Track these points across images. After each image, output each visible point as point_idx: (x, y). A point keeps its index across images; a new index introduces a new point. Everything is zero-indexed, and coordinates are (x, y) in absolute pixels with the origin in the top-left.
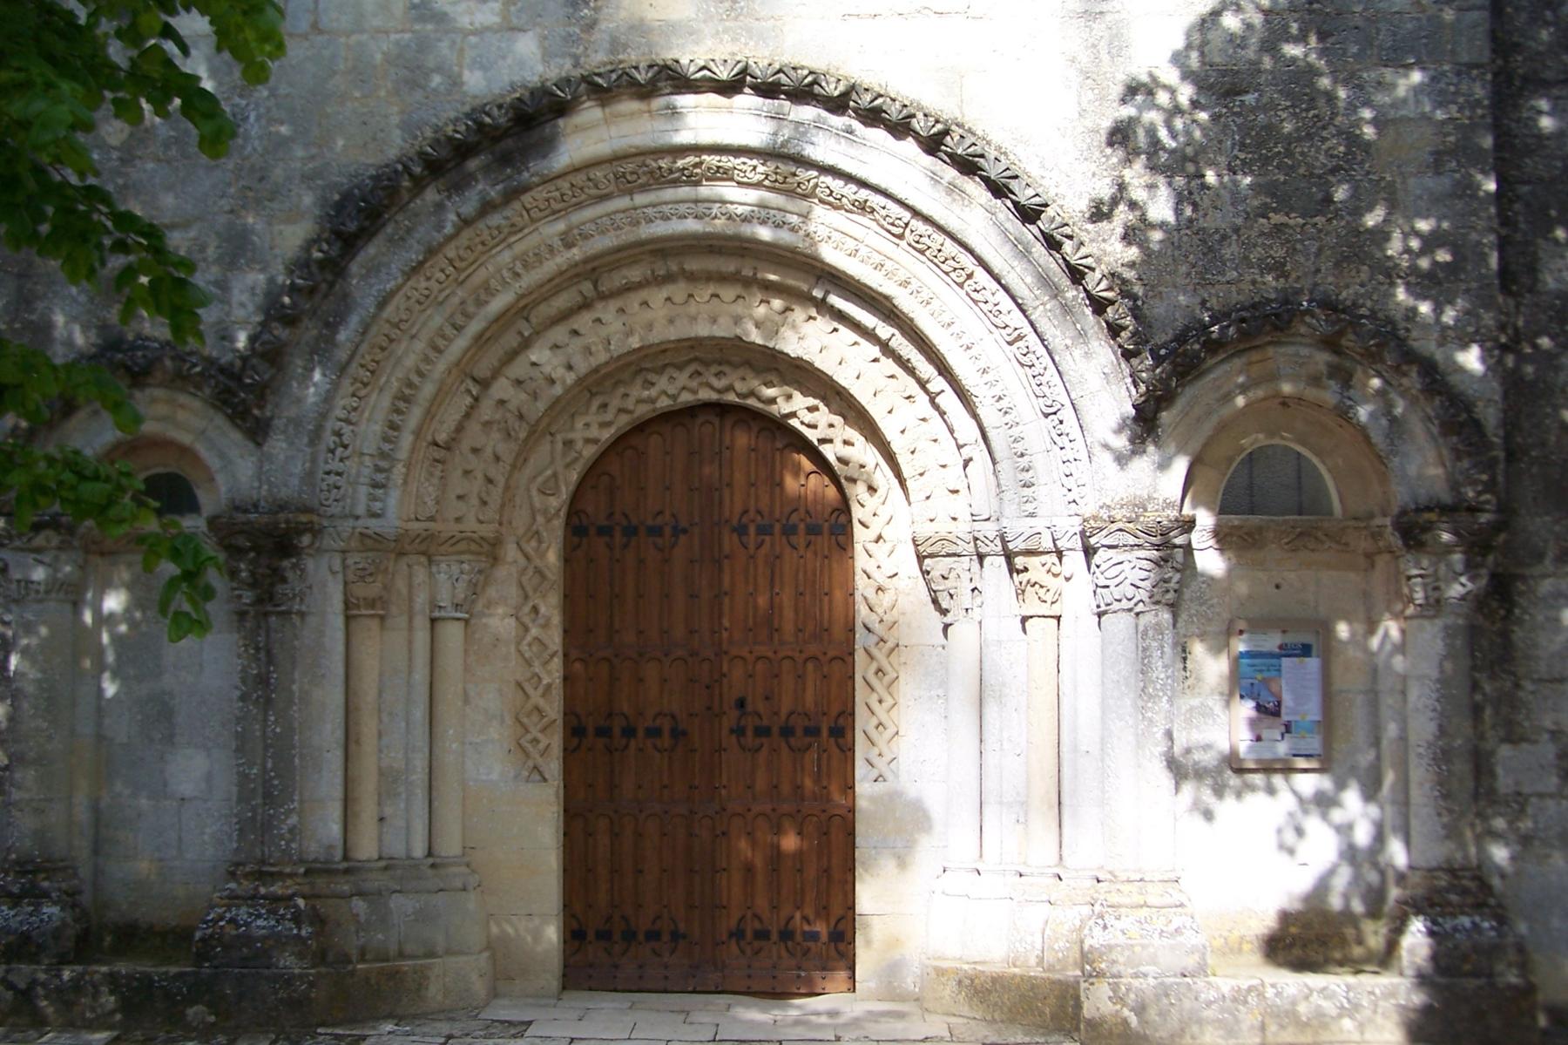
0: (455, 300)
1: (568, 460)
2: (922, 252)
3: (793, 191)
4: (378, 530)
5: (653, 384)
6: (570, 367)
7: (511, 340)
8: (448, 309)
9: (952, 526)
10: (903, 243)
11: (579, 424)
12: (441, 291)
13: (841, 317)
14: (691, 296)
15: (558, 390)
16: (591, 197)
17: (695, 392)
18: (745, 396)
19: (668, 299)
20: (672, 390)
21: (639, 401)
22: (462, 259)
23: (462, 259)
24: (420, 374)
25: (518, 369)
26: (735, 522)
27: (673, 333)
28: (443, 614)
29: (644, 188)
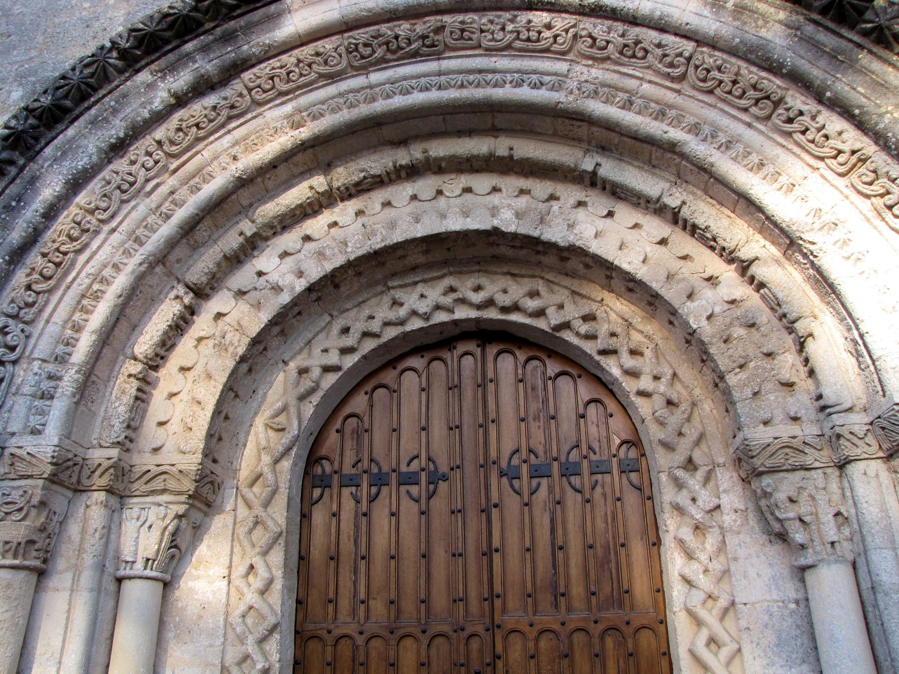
0: (164, 189)
1: (302, 390)
2: (711, 92)
3: (547, 50)
4: (33, 450)
5: (402, 305)
6: (300, 274)
7: (231, 241)
8: (155, 197)
9: (795, 429)
10: (685, 87)
11: (317, 351)
12: (148, 181)
13: (617, 192)
14: (440, 193)
15: (285, 298)
16: (321, 76)
17: (451, 311)
18: (505, 310)
19: (414, 197)
20: (423, 307)
21: (387, 324)
22: (172, 143)
23: (172, 143)
24: (116, 267)
25: (243, 277)
26: (504, 464)
27: (420, 231)
28: (128, 572)
29: (381, 63)
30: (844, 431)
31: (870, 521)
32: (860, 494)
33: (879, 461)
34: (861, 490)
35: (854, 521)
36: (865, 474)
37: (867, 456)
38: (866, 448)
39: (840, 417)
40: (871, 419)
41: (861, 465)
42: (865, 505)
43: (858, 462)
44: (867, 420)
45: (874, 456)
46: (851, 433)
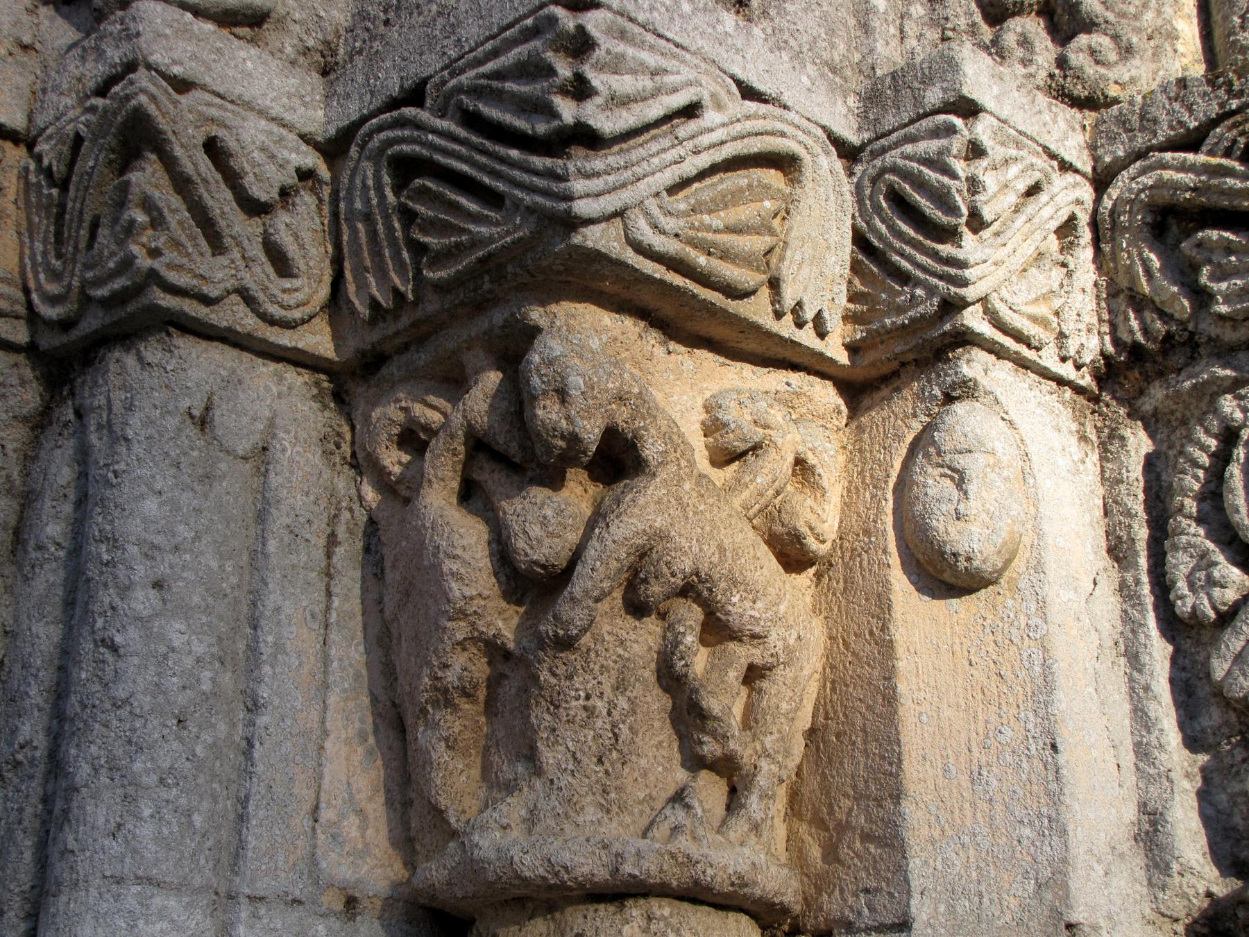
30: (183, 124)
31: (144, 701)
32: (133, 528)
33: (297, 379)
34: (151, 506)
35: (36, 695)
36: (203, 422)
37: (247, 322)
38: (260, 275)
39: (184, 32)
40: (354, 111)
41: (202, 364)
42: (143, 600)
43: (186, 345)
44: (317, 118)
45: (285, 339)
46: (212, 147)
